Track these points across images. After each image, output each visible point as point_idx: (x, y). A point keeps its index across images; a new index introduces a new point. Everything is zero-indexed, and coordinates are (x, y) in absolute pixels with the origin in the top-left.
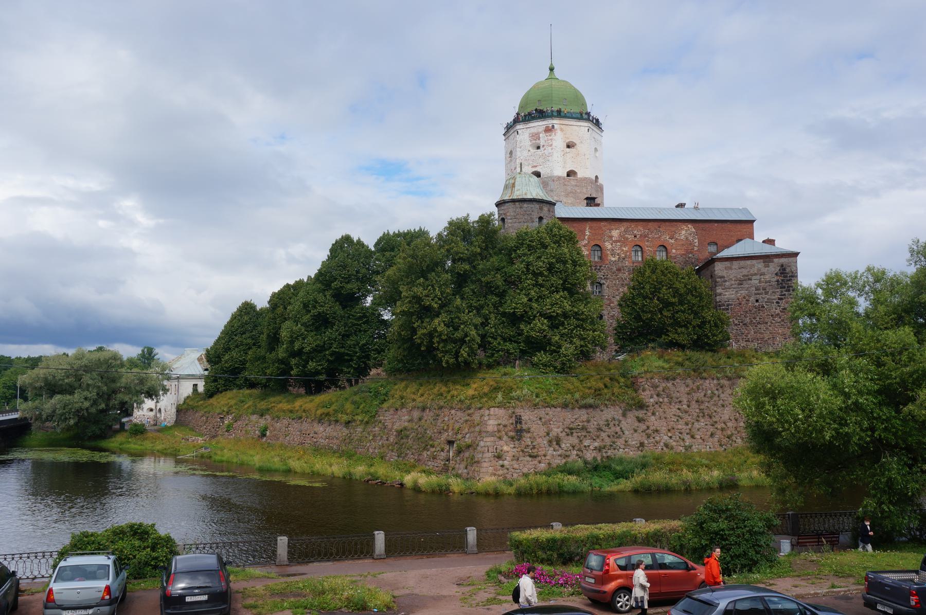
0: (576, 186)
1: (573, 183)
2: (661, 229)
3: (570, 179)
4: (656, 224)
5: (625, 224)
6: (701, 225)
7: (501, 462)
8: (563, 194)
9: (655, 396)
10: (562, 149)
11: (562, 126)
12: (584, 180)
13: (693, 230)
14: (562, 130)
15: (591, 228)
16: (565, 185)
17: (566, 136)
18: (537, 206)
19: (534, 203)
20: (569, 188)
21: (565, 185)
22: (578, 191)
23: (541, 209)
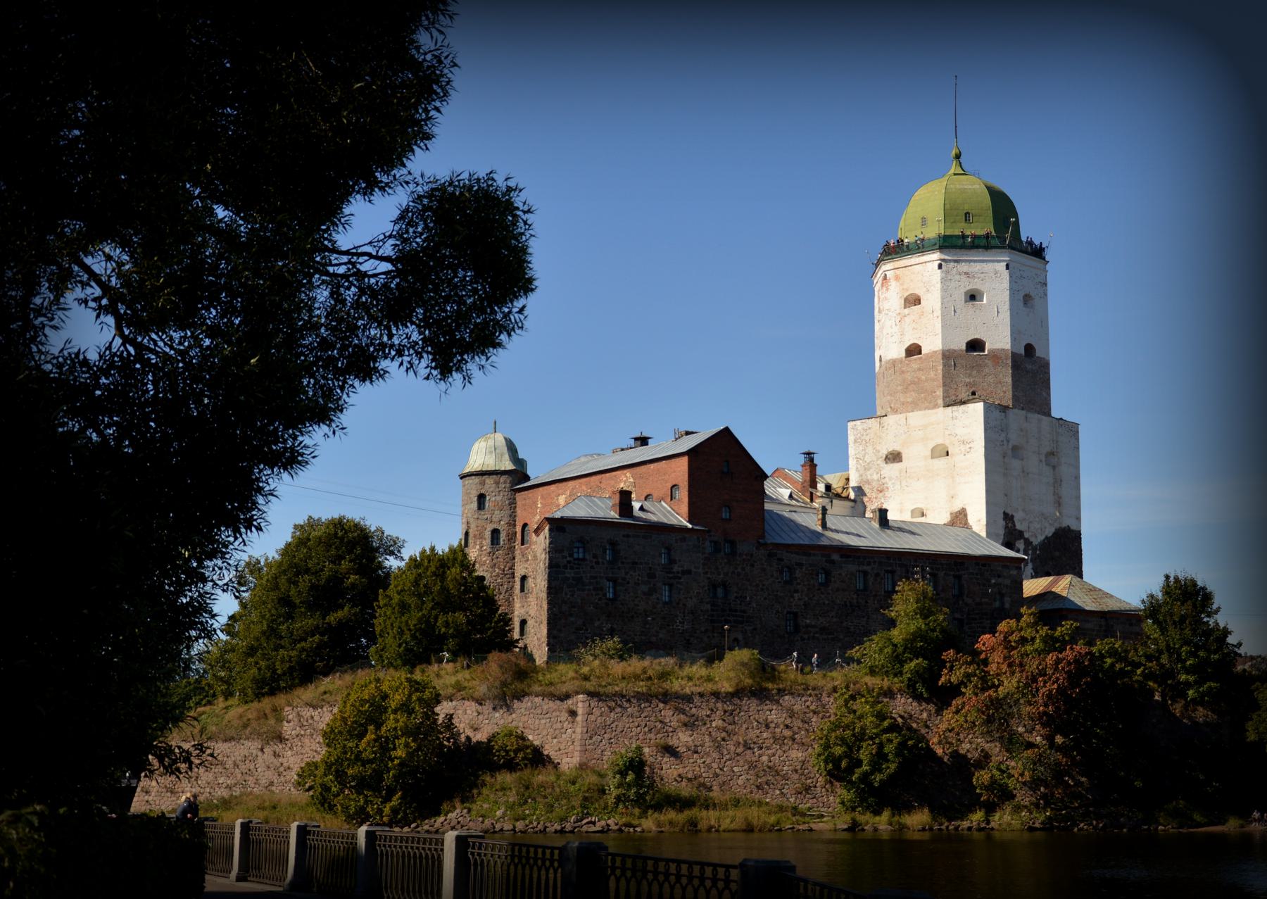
0: (919, 369)
1: (915, 366)
2: (602, 486)
3: (910, 361)
4: (598, 477)
5: (571, 484)
6: (638, 469)
7: (146, 798)
8: (899, 388)
9: (298, 728)
10: (898, 312)
11: (898, 272)
12: (931, 357)
13: (632, 480)
14: (897, 278)
15: (542, 497)
16: (903, 372)
17: (905, 287)
18: (476, 480)
19: (473, 477)
20: (909, 377)
21: (903, 372)
22: (923, 377)
23: (483, 483)
